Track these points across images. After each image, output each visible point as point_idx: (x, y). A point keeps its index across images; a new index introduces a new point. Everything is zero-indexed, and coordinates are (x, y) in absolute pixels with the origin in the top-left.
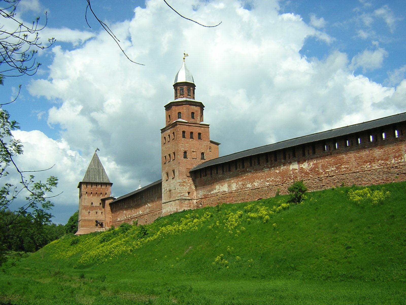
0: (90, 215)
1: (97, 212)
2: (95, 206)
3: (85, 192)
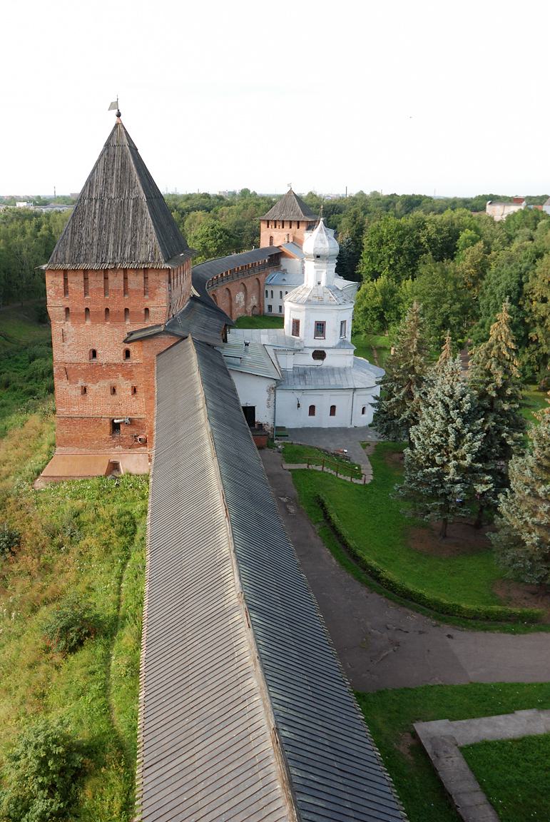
1: (114, 391)
2: (108, 365)
3: (62, 309)
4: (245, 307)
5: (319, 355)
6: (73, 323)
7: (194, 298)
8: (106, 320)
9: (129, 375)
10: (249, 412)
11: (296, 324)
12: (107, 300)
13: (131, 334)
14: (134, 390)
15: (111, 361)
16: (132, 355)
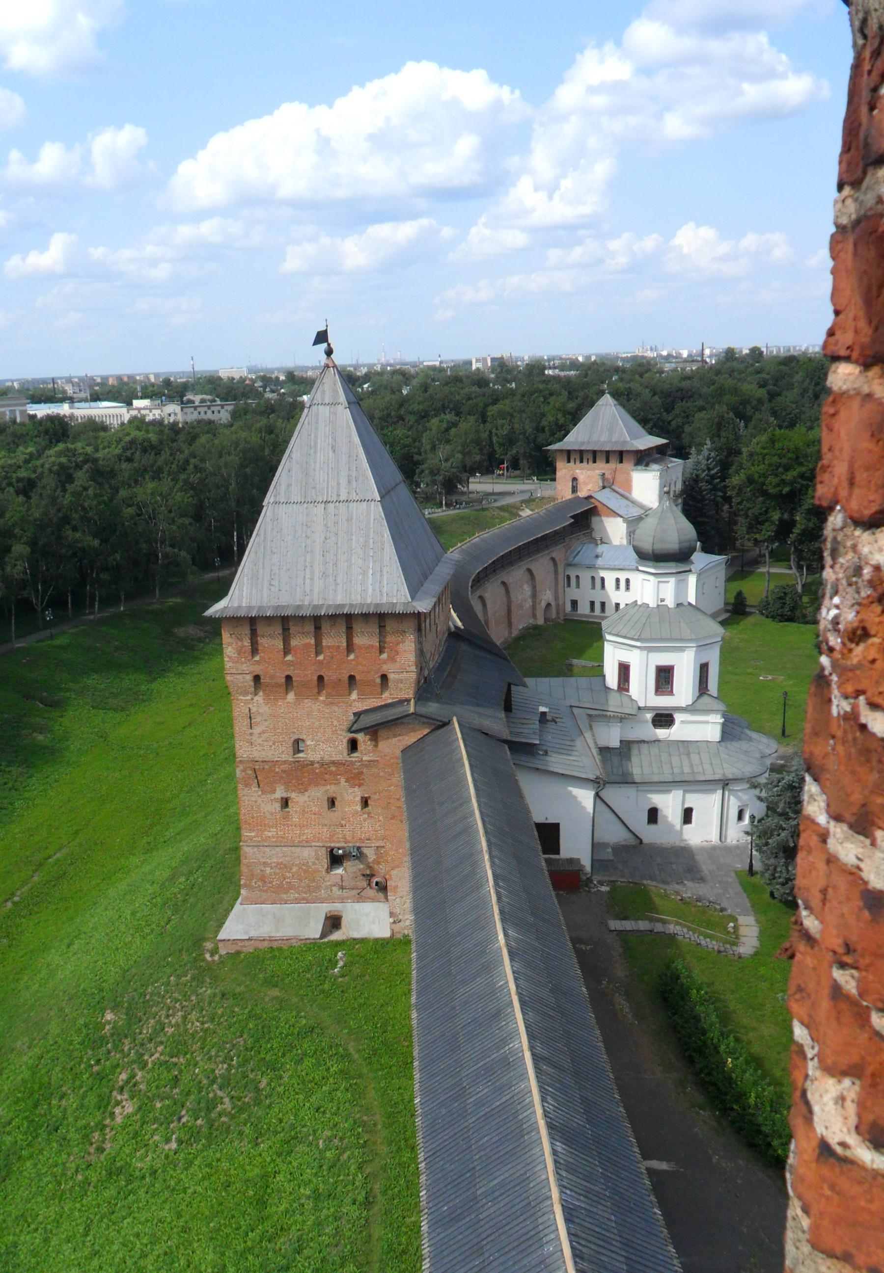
0: (295, 819)
1: (332, 803)
3: (249, 678)
4: (534, 607)
5: (664, 719)
6: (267, 699)
7: (455, 635)
8: (319, 693)
9: (356, 778)
10: (549, 834)
11: (624, 670)
12: (321, 662)
13: (358, 715)
14: (365, 802)
15: (327, 758)
16: (361, 746)
